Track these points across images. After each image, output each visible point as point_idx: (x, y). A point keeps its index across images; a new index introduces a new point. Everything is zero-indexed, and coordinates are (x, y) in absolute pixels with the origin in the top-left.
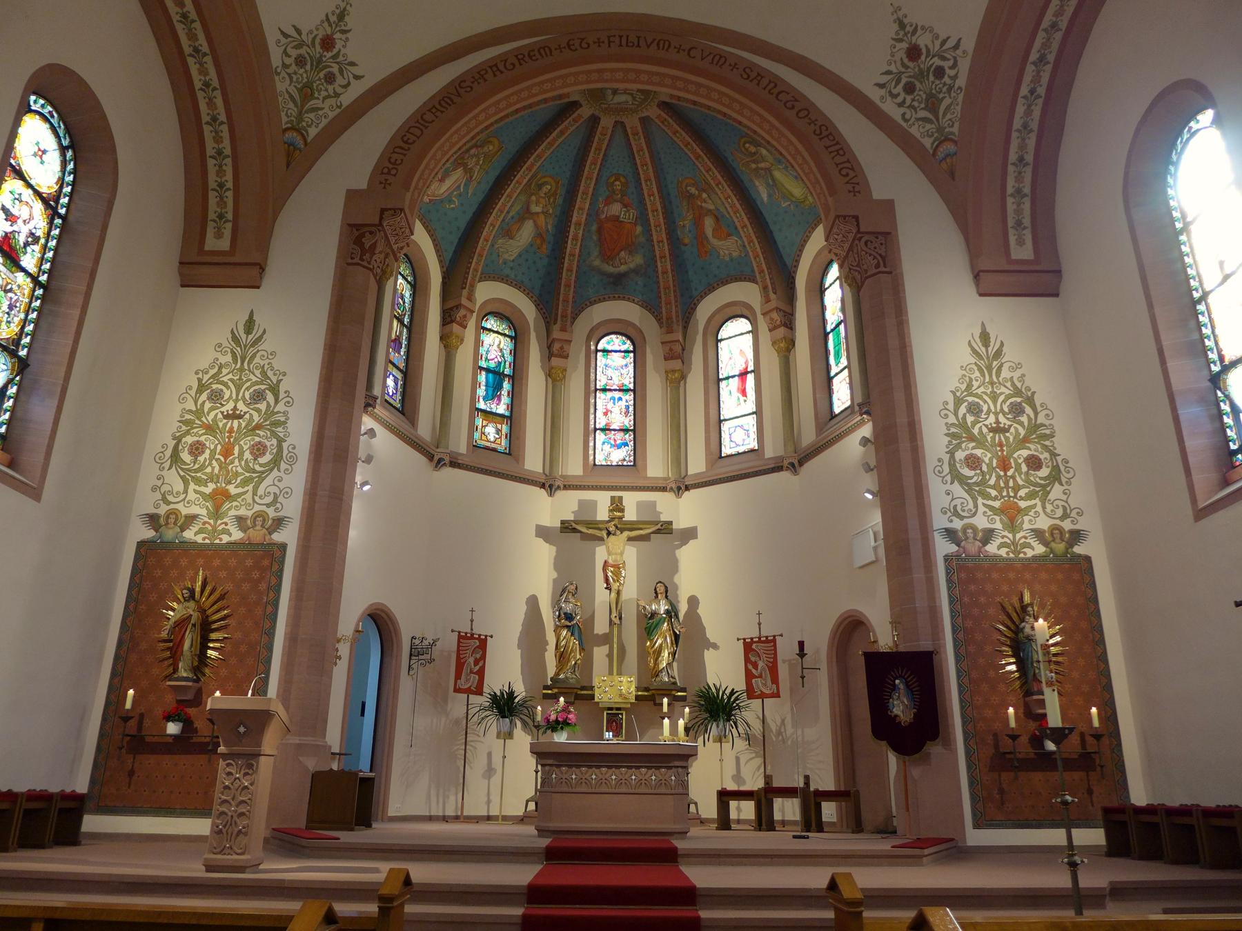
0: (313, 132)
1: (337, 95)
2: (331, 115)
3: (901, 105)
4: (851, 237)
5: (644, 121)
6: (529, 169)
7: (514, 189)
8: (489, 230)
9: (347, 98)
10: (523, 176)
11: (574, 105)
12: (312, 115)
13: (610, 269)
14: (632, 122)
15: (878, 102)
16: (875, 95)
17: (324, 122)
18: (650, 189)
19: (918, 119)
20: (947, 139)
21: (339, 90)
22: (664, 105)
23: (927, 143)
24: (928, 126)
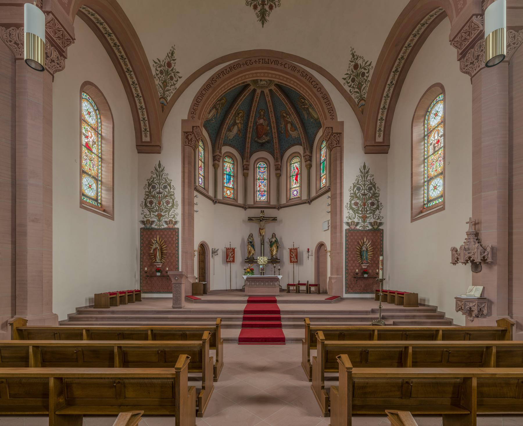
0: (169, 98)
1: (174, 84)
2: (174, 92)
3: (350, 86)
4: (330, 134)
5: (271, 90)
6: (235, 108)
7: (231, 116)
8: (224, 131)
9: (178, 85)
10: (233, 111)
11: (248, 86)
12: (168, 92)
13: (260, 141)
14: (266, 91)
15: (343, 85)
16: (342, 82)
17: (172, 95)
18: (272, 115)
19: (354, 92)
20: (363, 99)
21: (175, 83)
22: (277, 85)
23: (356, 100)
24: (357, 94)
